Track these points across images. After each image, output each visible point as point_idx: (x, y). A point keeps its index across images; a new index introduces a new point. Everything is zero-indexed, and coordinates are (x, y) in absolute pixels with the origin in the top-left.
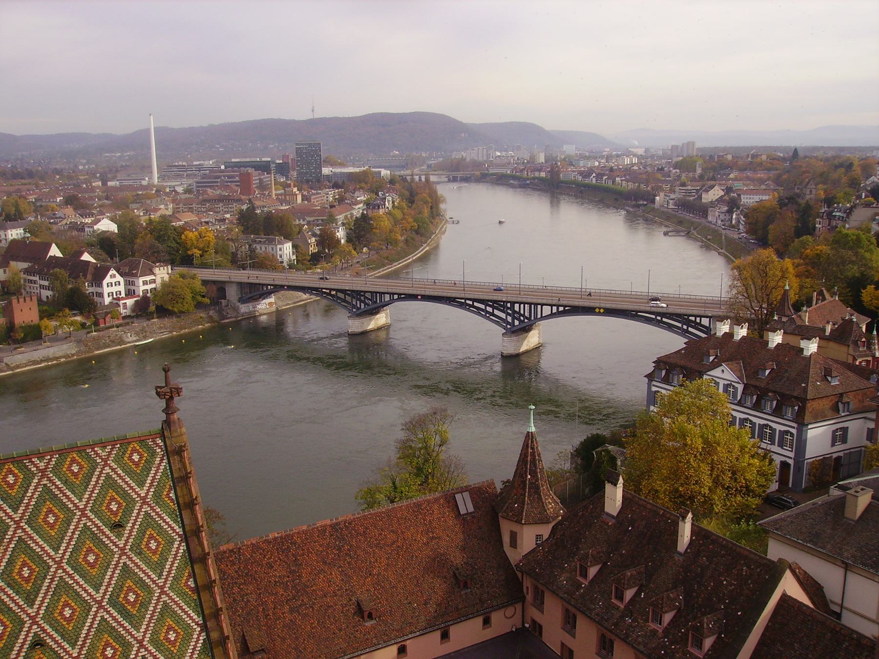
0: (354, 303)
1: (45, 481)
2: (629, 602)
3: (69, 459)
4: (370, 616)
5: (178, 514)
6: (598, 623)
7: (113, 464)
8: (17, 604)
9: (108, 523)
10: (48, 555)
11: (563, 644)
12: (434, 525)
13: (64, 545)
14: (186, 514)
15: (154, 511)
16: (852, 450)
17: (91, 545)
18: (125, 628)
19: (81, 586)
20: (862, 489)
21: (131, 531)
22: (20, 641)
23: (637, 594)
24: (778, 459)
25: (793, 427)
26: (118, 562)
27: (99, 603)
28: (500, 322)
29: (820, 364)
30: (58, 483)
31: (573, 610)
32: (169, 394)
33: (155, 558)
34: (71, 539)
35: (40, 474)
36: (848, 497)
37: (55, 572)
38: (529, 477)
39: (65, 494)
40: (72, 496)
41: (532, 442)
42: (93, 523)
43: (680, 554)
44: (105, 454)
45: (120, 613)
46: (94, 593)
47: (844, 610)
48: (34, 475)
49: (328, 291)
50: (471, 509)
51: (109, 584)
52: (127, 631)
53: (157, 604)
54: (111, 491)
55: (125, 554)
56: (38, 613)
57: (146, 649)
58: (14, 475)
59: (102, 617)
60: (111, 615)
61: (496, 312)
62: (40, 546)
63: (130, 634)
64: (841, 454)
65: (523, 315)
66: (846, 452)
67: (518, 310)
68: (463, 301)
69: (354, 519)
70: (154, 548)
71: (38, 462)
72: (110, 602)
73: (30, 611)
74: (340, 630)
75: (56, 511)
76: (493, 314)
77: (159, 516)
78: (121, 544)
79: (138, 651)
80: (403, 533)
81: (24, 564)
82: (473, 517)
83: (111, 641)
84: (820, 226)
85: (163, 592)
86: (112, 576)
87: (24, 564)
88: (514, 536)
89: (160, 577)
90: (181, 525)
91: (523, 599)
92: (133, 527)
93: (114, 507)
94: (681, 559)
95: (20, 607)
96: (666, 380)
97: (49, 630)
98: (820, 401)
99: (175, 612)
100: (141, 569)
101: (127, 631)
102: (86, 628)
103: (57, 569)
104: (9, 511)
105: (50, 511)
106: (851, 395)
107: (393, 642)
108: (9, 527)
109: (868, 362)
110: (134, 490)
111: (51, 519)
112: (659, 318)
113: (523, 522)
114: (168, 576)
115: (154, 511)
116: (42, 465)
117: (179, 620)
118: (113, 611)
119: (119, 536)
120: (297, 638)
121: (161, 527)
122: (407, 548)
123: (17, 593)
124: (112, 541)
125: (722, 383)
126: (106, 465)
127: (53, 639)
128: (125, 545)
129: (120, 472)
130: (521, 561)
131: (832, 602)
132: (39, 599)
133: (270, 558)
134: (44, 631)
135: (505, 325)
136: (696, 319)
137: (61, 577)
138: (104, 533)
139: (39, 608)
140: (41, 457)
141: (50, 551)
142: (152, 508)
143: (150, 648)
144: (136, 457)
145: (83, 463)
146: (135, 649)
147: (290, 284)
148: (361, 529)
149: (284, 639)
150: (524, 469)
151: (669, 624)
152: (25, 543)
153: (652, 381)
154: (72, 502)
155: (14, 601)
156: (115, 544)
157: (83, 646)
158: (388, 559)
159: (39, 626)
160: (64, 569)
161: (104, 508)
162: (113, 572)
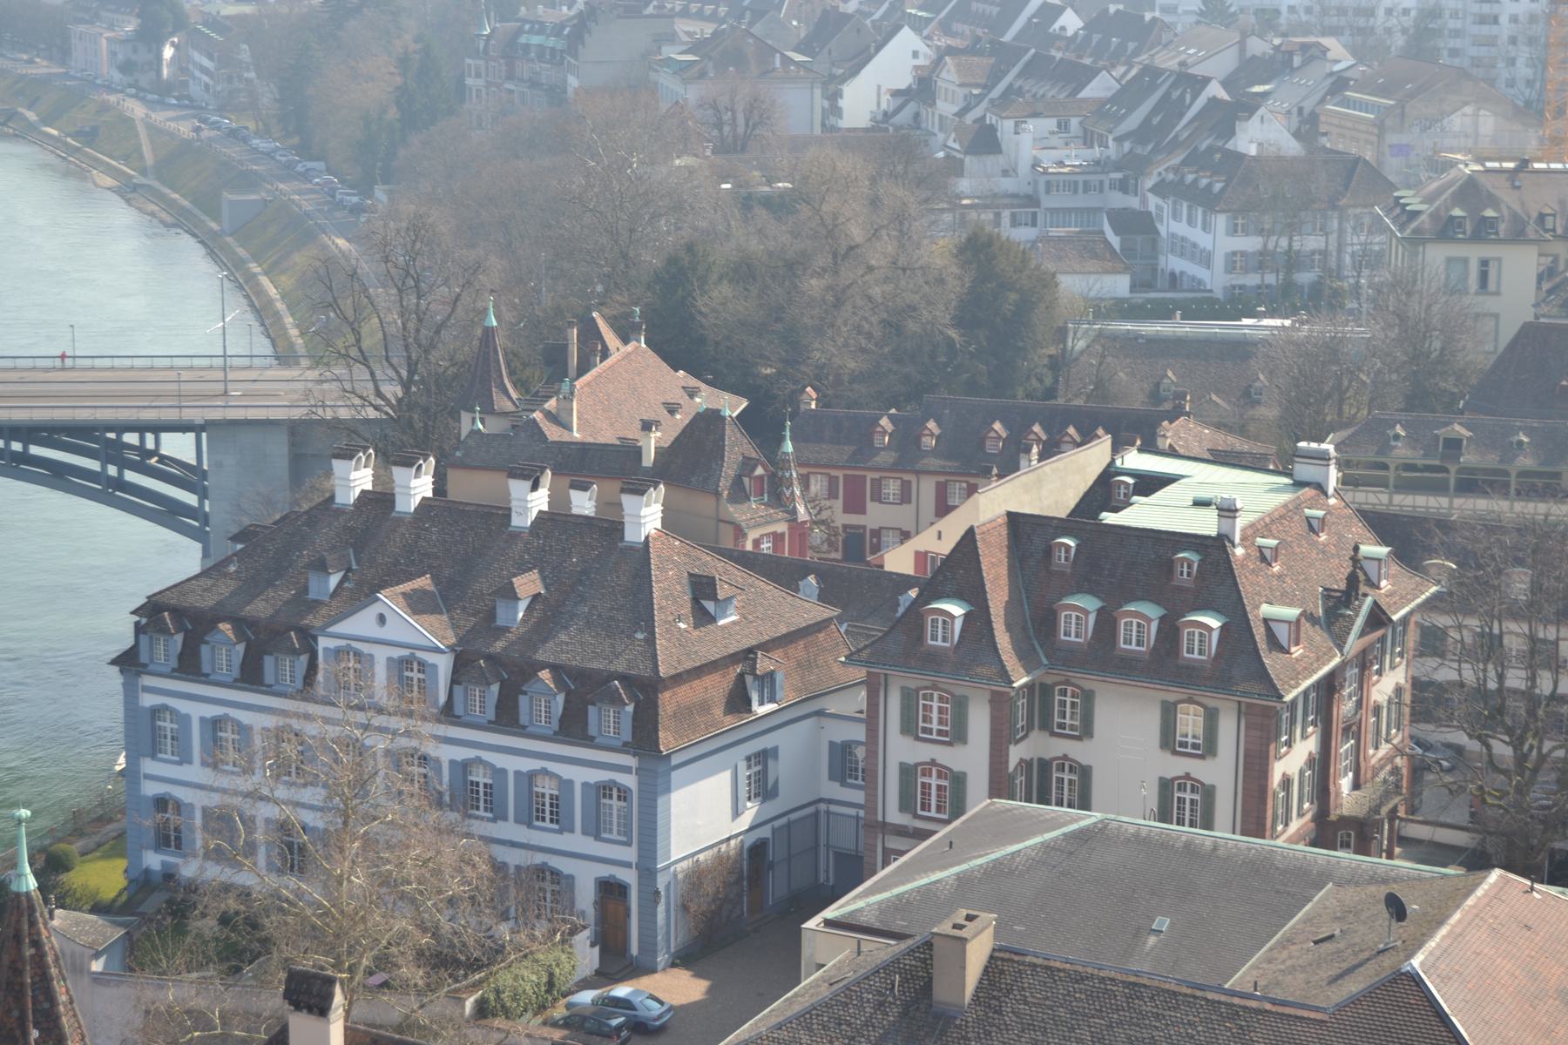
16: (793, 816)
24: (586, 880)
25: (626, 770)
36: (937, 942)
64: (765, 832)
66: (777, 823)
84: (481, 82)
96: (189, 666)
109: (777, 538)
112: (17, 446)
125: (381, 655)
136: (142, 440)
150: (16, 1013)
153: (138, 674)
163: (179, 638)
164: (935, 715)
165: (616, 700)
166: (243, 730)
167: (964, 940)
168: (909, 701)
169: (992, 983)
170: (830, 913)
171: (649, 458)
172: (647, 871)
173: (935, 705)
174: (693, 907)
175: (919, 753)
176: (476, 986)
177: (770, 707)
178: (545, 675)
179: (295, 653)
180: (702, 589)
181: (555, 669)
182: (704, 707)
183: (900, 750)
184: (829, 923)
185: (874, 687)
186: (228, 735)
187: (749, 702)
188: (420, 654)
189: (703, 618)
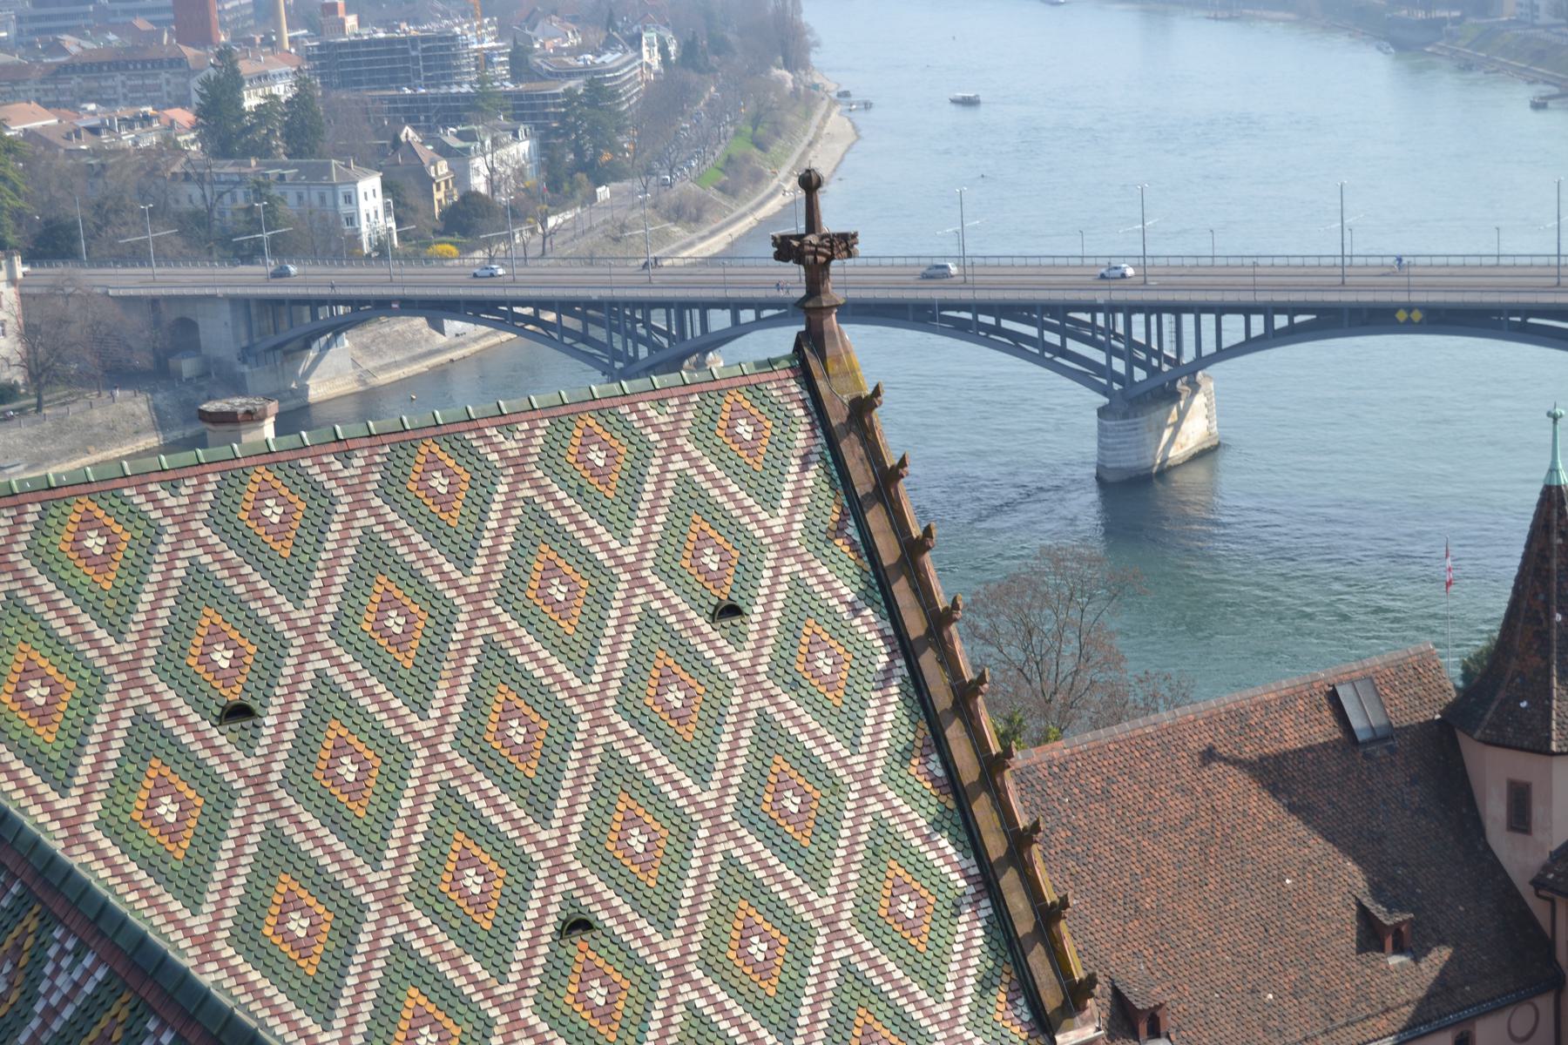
0: (618, 346)
1: (526, 491)
5: (874, 581)
9: (704, 603)
18: (787, 886)
28: (1088, 374)
30: (561, 495)
32: (825, 250)
34: (616, 644)
35: (511, 471)
37: (591, 733)
38: (1559, 617)
40: (600, 530)
44: (666, 419)
49: (528, 311)
58: (445, 472)
61: (1072, 345)
65: (1158, 354)
67: (1143, 341)
68: (967, 316)
69: (1072, 754)
71: (501, 438)
72: (739, 814)
76: (1063, 352)
80: (1208, 793)
82: (1392, 750)
85: (868, 790)
89: (854, 745)
90: (885, 611)
93: (711, 561)
97: (599, 887)
104: (448, 567)
113: (1554, 747)
118: (750, 839)
119: (737, 638)
123: (506, 787)
126: (673, 448)
129: (711, 468)
130: (1546, 868)
132: (562, 803)
135: (1104, 381)
140: (508, 428)
141: (568, 676)
144: (744, 430)
147: (408, 292)
148: (1095, 783)
150: (1541, 597)
154: (604, 546)
158: (1179, 865)
160: (609, 725)
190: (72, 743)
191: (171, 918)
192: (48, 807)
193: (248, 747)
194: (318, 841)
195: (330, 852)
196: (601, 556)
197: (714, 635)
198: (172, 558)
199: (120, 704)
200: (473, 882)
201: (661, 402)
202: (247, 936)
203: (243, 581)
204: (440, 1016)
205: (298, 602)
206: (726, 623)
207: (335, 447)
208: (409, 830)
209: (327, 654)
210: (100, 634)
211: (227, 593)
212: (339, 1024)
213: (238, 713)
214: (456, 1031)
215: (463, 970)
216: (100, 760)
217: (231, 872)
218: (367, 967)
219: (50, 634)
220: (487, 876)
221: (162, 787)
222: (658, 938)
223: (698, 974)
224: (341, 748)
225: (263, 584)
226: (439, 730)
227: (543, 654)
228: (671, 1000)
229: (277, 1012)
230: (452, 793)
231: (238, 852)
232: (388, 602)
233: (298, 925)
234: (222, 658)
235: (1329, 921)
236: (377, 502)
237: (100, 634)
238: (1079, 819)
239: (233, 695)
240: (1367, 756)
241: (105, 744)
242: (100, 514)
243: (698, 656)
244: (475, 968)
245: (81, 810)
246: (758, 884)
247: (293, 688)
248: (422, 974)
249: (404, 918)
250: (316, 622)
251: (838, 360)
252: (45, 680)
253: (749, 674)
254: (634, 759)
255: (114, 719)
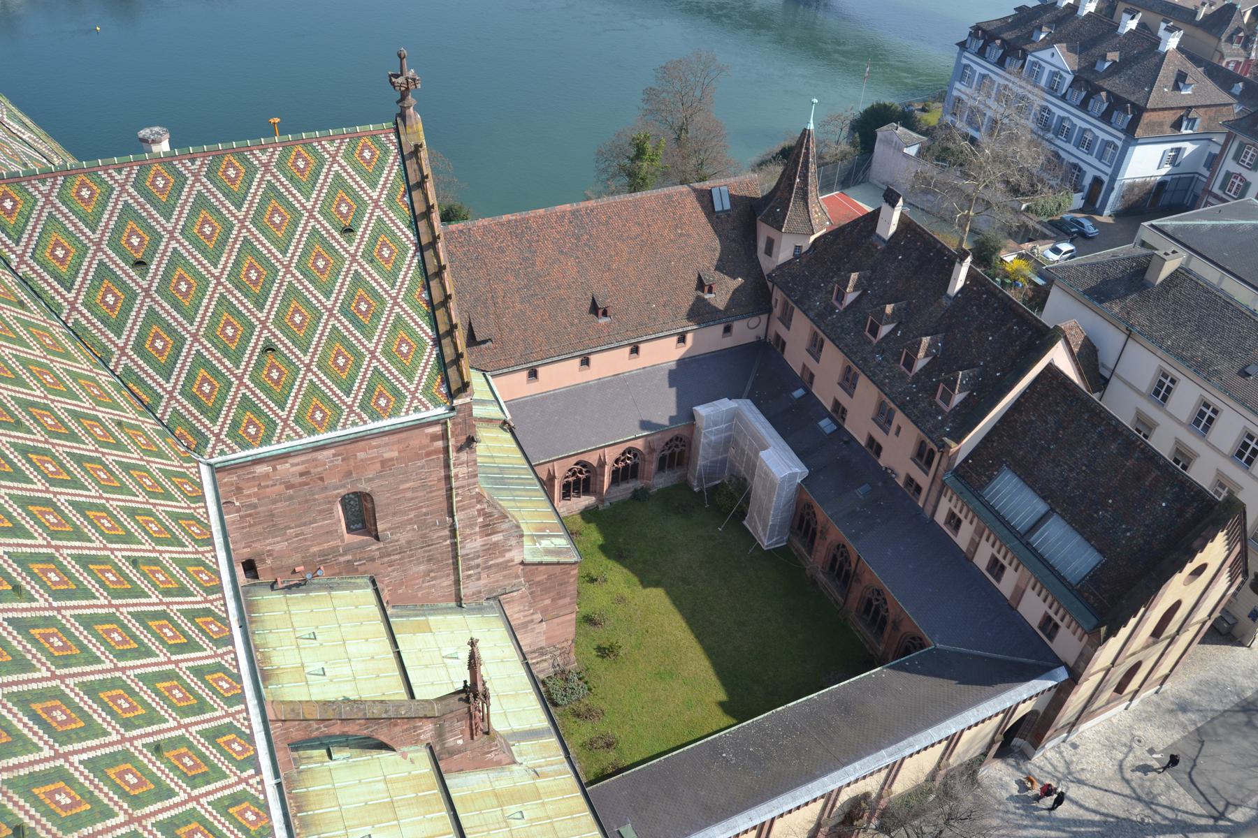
1: (268, 177)
2: (883, 338)
3: (294, 153)
4: (605, 314)
6: (845, 354)
7: (342, 161)
8: (246, 307)
10: (276, 258)
11: (804, 366)
12: (685, 220)
13: (292, 248)
14: (422, 225)
15: (387, 216)
17: (321, 250)
18: (356, 338)
19: (311, 293)
20: (1174, 252)
21: (362, 237)
22: (251, 345)
23: (894, 331)
25: (1120, 139)
26: (349, 270)
27: (330, 310)
29: (1175, 65)
30: (283, 179)
31: (821, 334)
33: (388, 267)
34: (299, 243)
36: (1155, 257)
37: (284, 277)
38: (798, 180)
39: (290, 193)
41: (808, 141)
42: (322, 226)
43: (949, 297)
45: (351, 321)
46: (324, 300)
47: (1113, 377)
48: (256, 169)
50: (727, 206)
51: (340, 291)
52: (359, 341)
53: (389, 315)
54: (340, 191)
55: (356, 261)
56: (268, 318)
57: (378, 360)
58: (235, 168)
59: (333, 325)
60: (342, 324)
62: (267, 248)
63: (362, 344)
64: (1168, 178)
70: (387, 256)
73: (260, 315)
74: (572, 325)
75: (282, 211)
77: (393, 222)
78: (352, 250)
79: (370, 362)
81: (251, 267)
82: (729, 215)
83: (343, 350)
85: (396, 303)
86: (343, 284)
87: (251, 267)
88: (770, 244)
89: (393, 286)
91: (769, 311)
92: (364, 233)
93: (344, 209)
94: (949, 302)
95: (249, 310)
96: (981, 53)
97: (280, 335)
98: (1160, 113)
99: (408, 325)
100: (373, 278)
101: (359, 341)
102: (317, 336)
103: (286, 273)
105: (275, 210)
106: (1201, 111)
107: (626, 342)
108: (232, 226)
109: (1238, 63)
110: (365, 192)
111: (277, 219)
114: (401, 287)
115: (387, 216)
116: (264, 158)
117: (412, 333)
118: (344, 320)
119: (350, 241)
120: (526, 330)
121: (395, 234)
122: (652, 244)
123: (246, 296)
124: (342, 247)
125: (1048, 68)
126: (334, 161)
127: (285, 345)
128: (356, 251)
129: (350, 170)
130: (773, 271)
131: (1103, 366)
132: (269, 303)
133: (502, 242)
134: (275, 336)
137: (290, 282)
138: (333, 238)
139: (269, 313)
140: (263, 150)
141: (277, 254)
142: (385, 213)
143: (383, 359)
144: (367, 154)
145: (309, 158)
146: (367, 359)
149: (512, 330)
151: (921, 370)
152: (251, 244)
154: (299, 202)
155: (243, 304)
156: (345, 249)
157: (314, 353)
158: (629, 253)
159: (270, 331)
161: (333, 210)
162: (344, 280)
163: (981, 42)
164: (1249, 156)
165: (1126, 112)
166: (993, 82)
167: (1165, 260)
168: (1242, 146)
169: (1171, 280)
170: (1155, 222)
171: (1200, 16)
172: (1113, 179)
173: (1251, 152)
174: (1126, 197)
175: (1237, 169)
176: (1026, 201)
177: (1190, 132)
178: (1103, 94)
179: (1019, 59)
180: (1181, 78)
181: (1109, 93)
182: (1161, 124)
183: (1229, 165)
184: (1152, 226)
185: (1229, 138)
186: (987, 82)
187: (1181, 127)
188: (1062, 72)
189: (1176, 87)
190: (73, 273)
191: (110, 340)
192: (63, 297)
193: (143, 277)
194: (169, 314)
195: (173, 317)
196: (297, 205)
197: (341, 240)
198: (117, 200)
199: (93, 259)
200: (230, 331)
201: (332, 141)
202: (139, 348)
203: (145, 210)
204: (212, 380)
205: (168, 221)
206: (347, 235)
207: (189, 156)
208: (206, 311)
209: (178, 241)
210: (86, 230)
211: (139, 216)
212: (172, 381)
213: (140, 264)
214: (218, 386)
215: (223, 364)
216: (84, 279)
217: (134, 324)
218: (185, 361)
219: (66, 229)
220: (236, 330)
221: (108, 290)
222: (301, 355)
223: (315, 369)
224: (181, 278)
225: (154, 212)
226: (222, 273)
227: (268, 244)
228: (304, 379)
229: (148, 375)
230: (224, 297)
231: (137, 316)
232: (205, 221)
233: (159, 344)
234: (135, 241)
235: (684, 279)
236: (204, 180)
237: (86, 230)
238: (594, 232)
239: (138, 256)
240: (717, 217)
241: (86, 274)
242: (88, 181)
243: (333, 248)
244: (227, 363)
245: (76, 298)
246: (345, 337)
247: (163, 254)
248: (206, 364)
249: (201, 344)
250: (175, 228)
251: (412, 127)
252: (63, 248)
253: (353, 256)
254: (300, 288)
255: (90, 263)
